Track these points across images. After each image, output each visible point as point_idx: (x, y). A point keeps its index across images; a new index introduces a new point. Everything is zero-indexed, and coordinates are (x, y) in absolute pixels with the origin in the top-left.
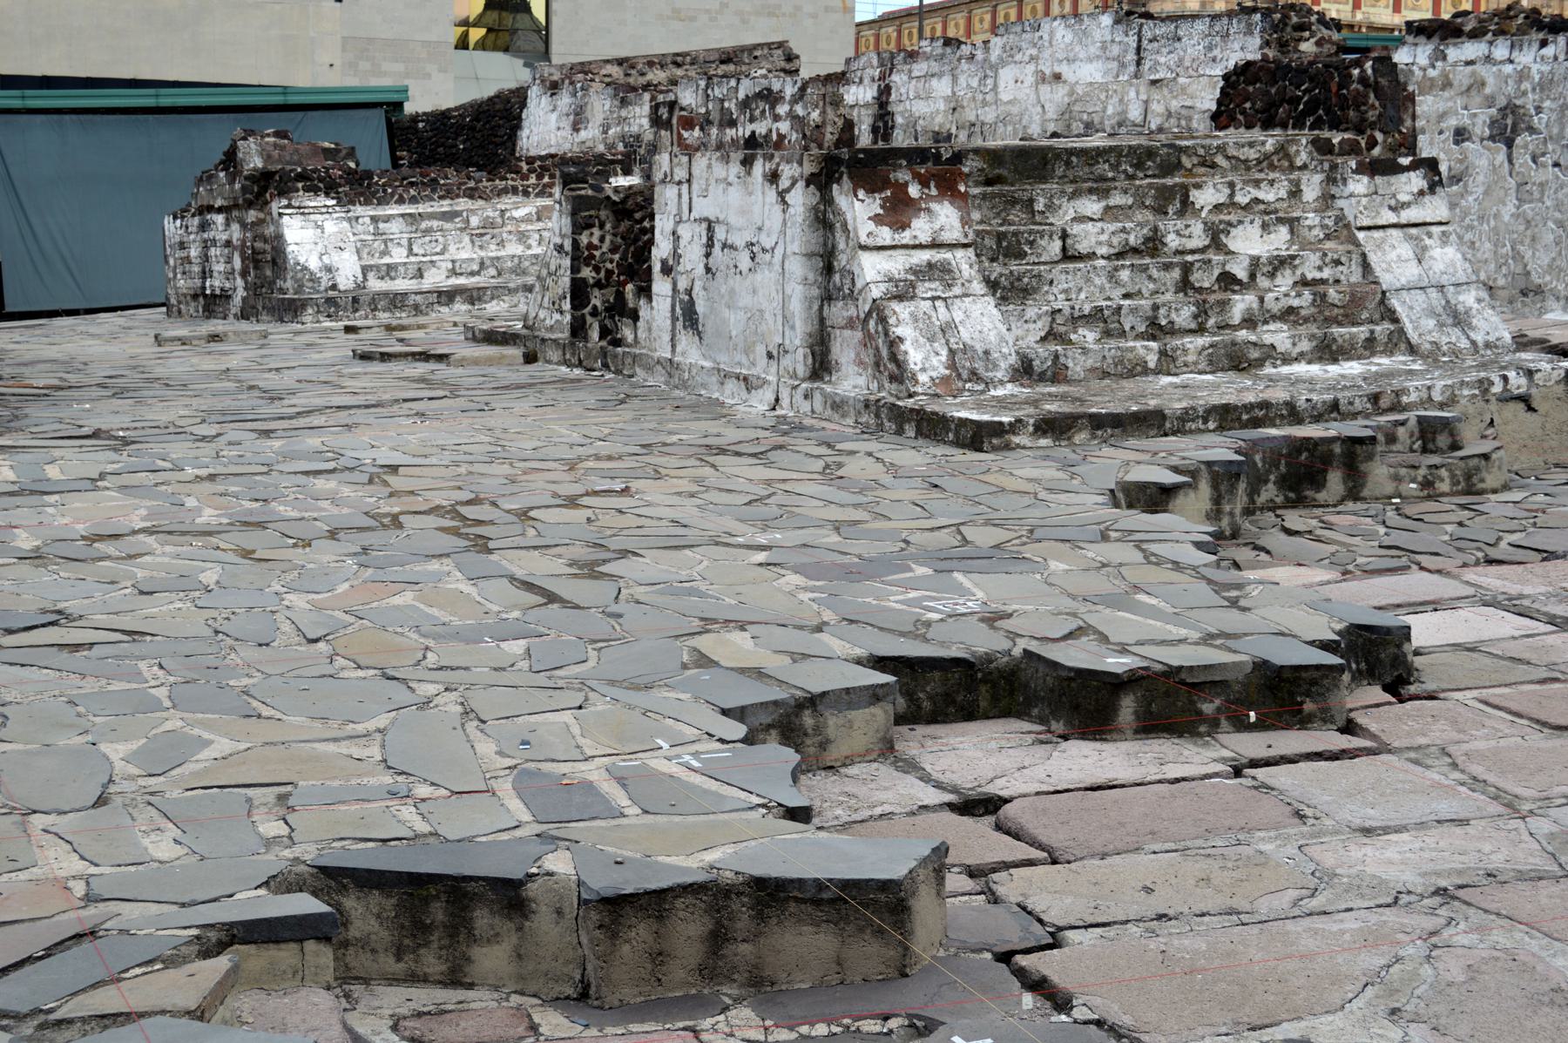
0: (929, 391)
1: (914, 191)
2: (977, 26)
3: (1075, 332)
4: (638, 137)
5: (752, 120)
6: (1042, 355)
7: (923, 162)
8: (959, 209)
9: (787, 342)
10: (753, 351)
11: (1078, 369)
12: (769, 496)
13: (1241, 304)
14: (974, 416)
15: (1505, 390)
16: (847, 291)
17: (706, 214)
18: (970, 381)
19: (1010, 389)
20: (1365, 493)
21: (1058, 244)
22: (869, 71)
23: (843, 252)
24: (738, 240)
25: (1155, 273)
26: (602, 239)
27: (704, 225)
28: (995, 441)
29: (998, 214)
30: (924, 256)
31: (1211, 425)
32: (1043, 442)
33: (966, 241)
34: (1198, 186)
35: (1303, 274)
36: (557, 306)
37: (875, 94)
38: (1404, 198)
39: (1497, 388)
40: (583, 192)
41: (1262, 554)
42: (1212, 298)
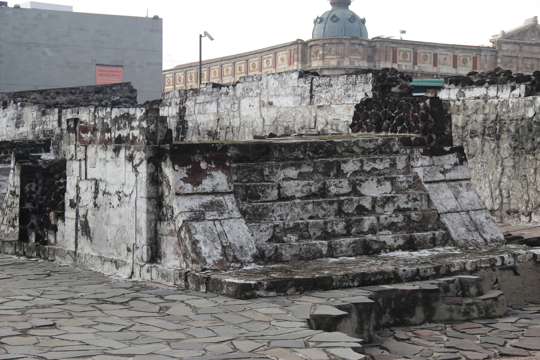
0: (213, 268)
1: (203, 165)
2: (225, 74)
3: (286, 236)
4: (52, 131)
5: (119, 129)
6: (269, 248)
7: (207, 152)
8: (226, 174)
9: (138, 242)
10: (120, 248)
11: (288, 255)
12: (132, 326)
13: (368, 221)
14: (236, 281)
15: (503, 264)
16: (169, 217)
17: (94, 177)
18: (233, 262)
19: (253, 266)
20: (435, 318)
21: (276, 192)
22: (174, 100)
23: (167, 196)
24: (112, 190)
25: (325, 206)
26: (37, 188)
27: (93, 182)
28: (247, 294)
29: (246, 177)
30: (208, 199)
31: (356, 284)
32: (272, 294)
33: (230, 191)
34: (345, 162)
35: (398, 206)
36: (11, 224)
37: (178, 111)
38: (447, 167)
39: (499, 263)
40: (26, 164)
41: (385, 351)
42: (354, 218)
